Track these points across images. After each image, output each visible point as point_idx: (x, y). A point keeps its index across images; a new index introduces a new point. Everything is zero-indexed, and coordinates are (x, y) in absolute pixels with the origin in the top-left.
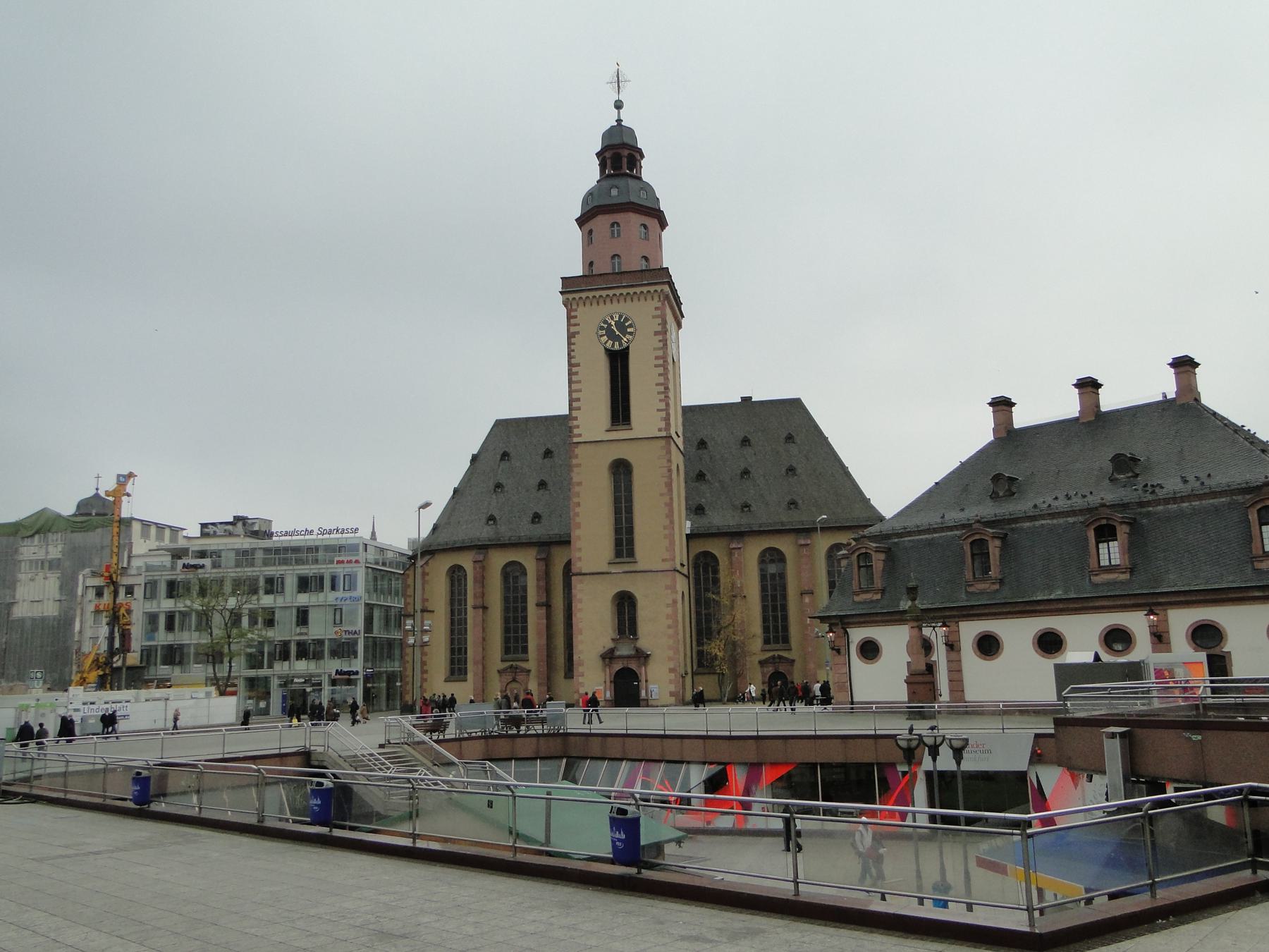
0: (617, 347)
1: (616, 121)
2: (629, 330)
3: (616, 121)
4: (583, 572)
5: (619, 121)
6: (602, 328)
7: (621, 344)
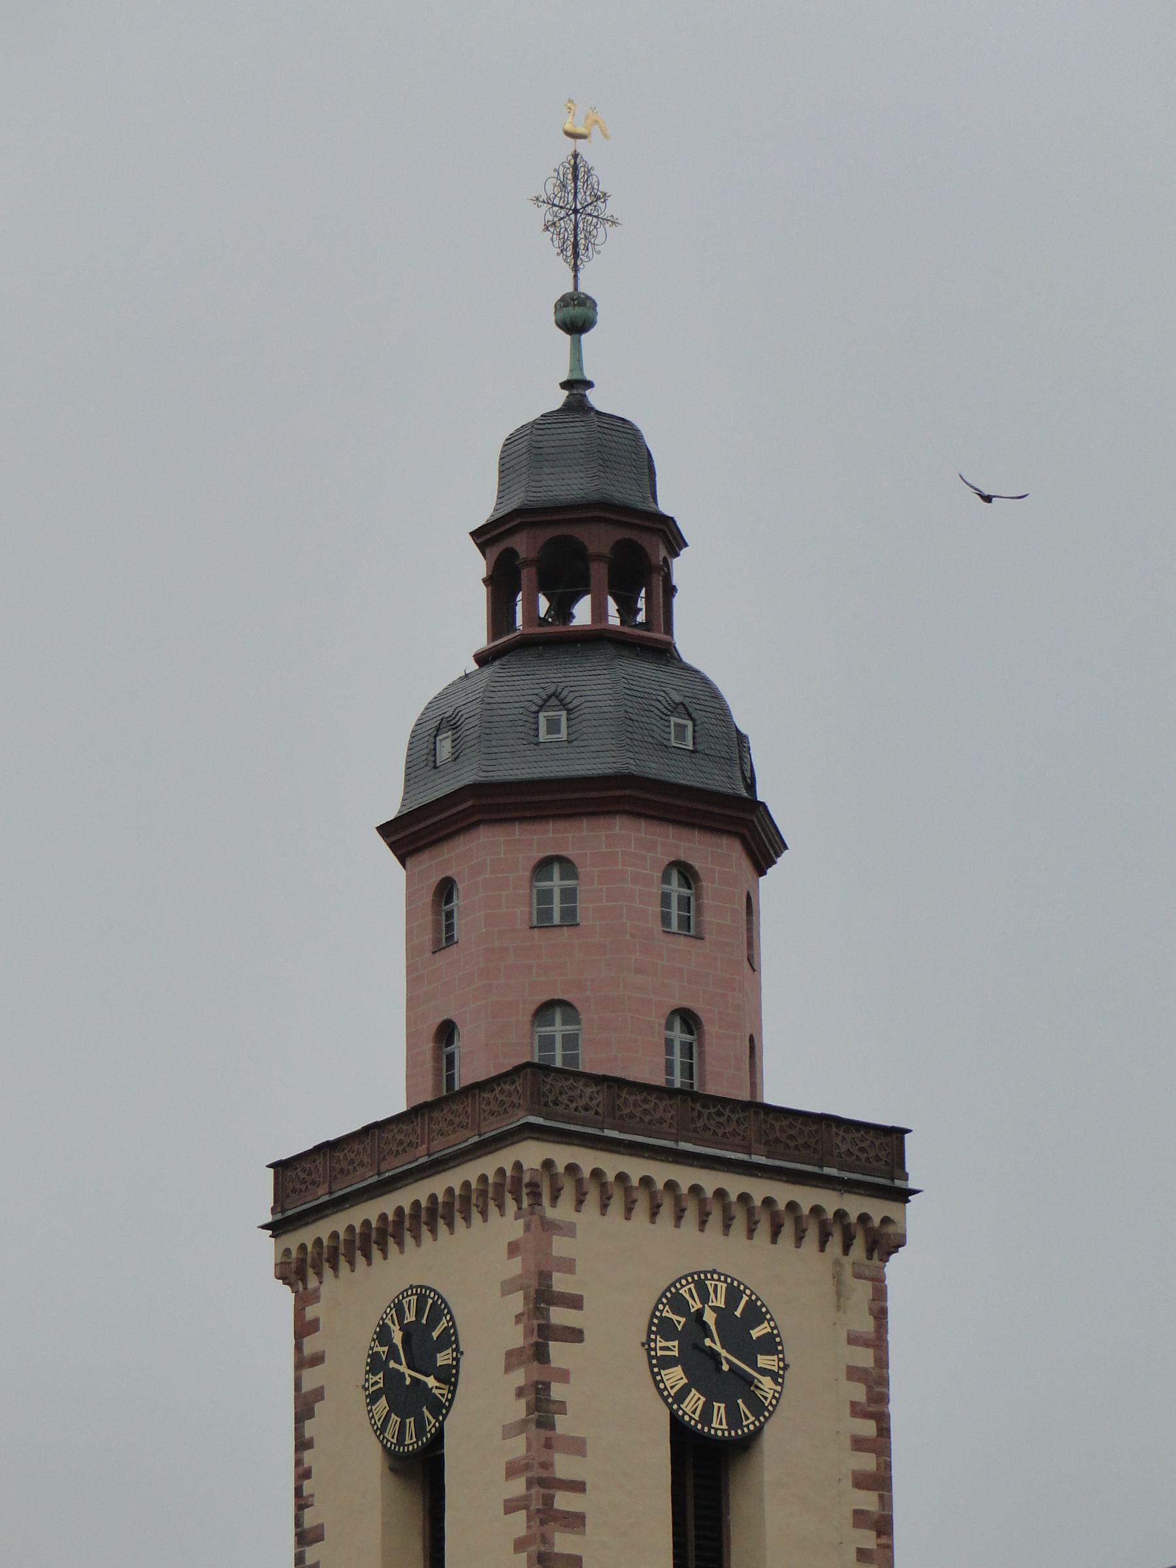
0: (719, 1425)
1: (565, 385)
2: (763, 1361)
3: (565, 385)
5: (576, 385)
6: (666, 1329)
7: (734, 1418)
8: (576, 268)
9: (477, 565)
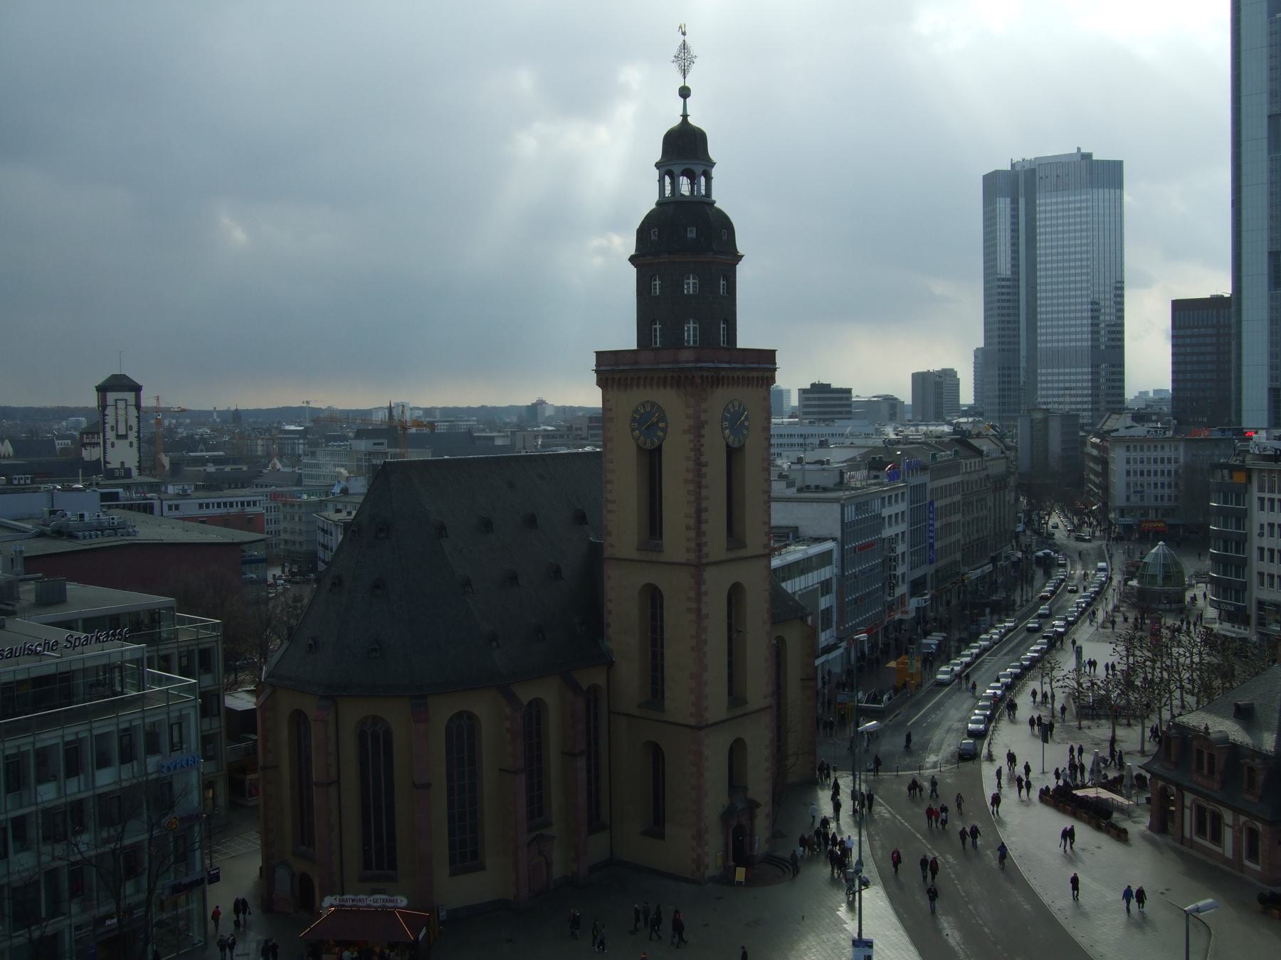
0: (736, 445)
4: (710, 722)
5: (685, 116)
8: (685, 78)
9: (655, 173)
